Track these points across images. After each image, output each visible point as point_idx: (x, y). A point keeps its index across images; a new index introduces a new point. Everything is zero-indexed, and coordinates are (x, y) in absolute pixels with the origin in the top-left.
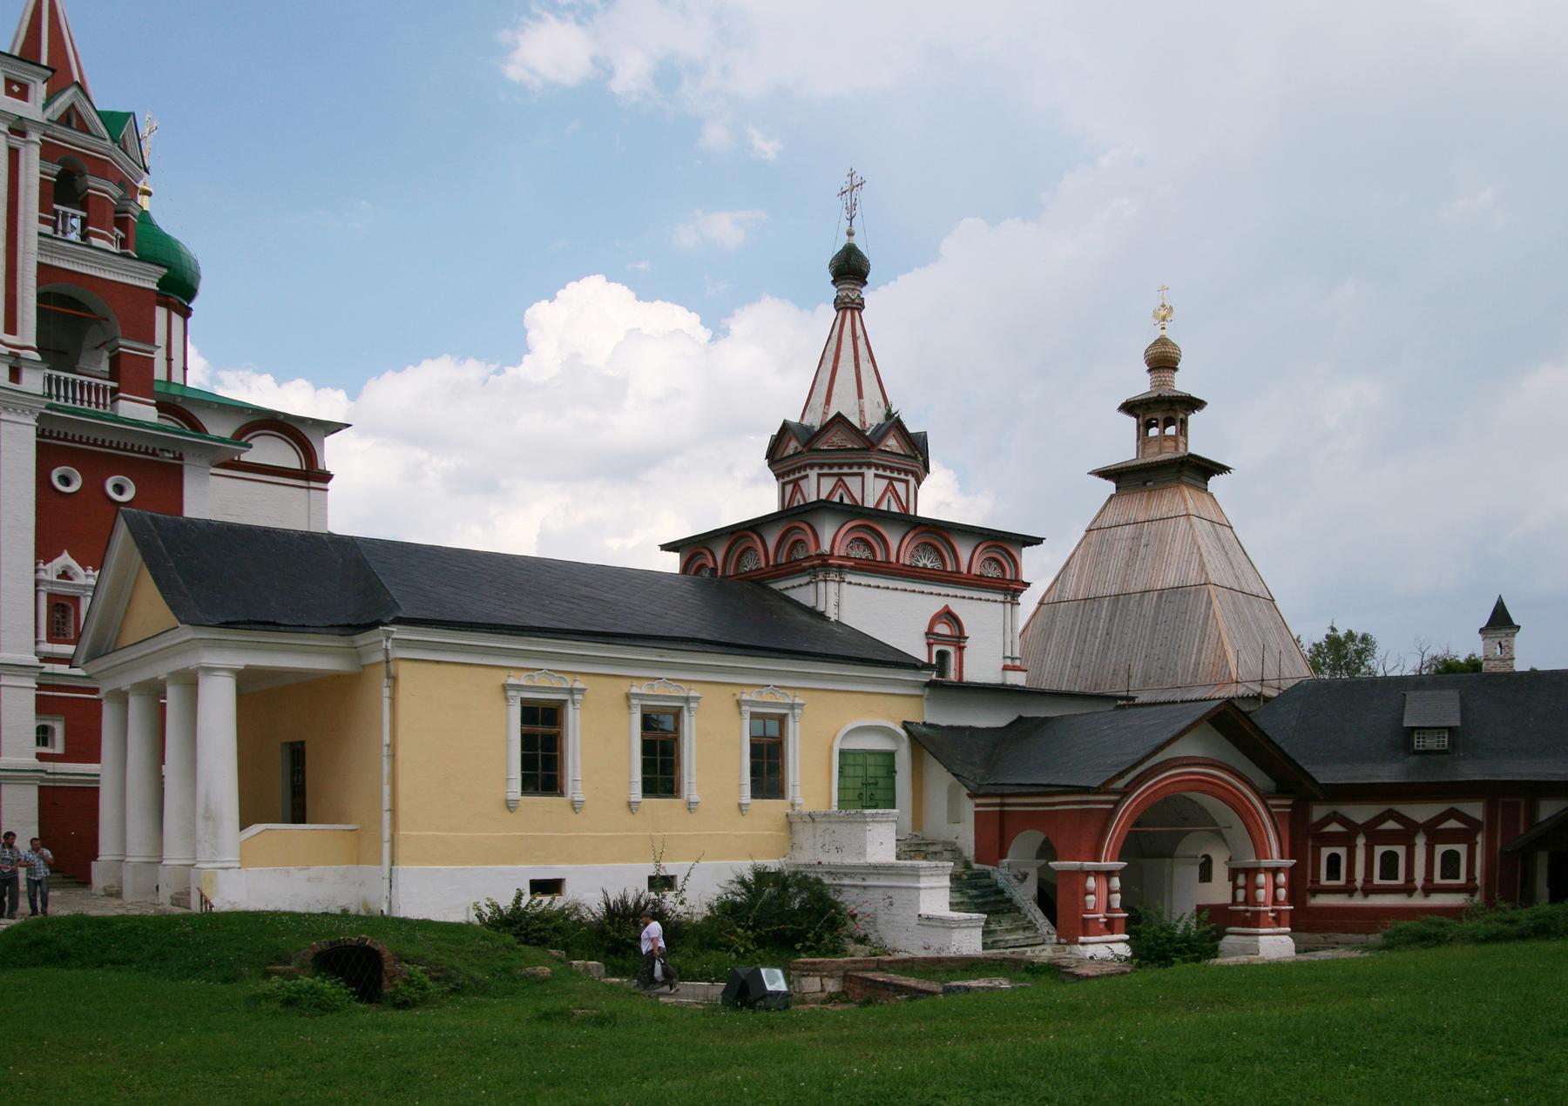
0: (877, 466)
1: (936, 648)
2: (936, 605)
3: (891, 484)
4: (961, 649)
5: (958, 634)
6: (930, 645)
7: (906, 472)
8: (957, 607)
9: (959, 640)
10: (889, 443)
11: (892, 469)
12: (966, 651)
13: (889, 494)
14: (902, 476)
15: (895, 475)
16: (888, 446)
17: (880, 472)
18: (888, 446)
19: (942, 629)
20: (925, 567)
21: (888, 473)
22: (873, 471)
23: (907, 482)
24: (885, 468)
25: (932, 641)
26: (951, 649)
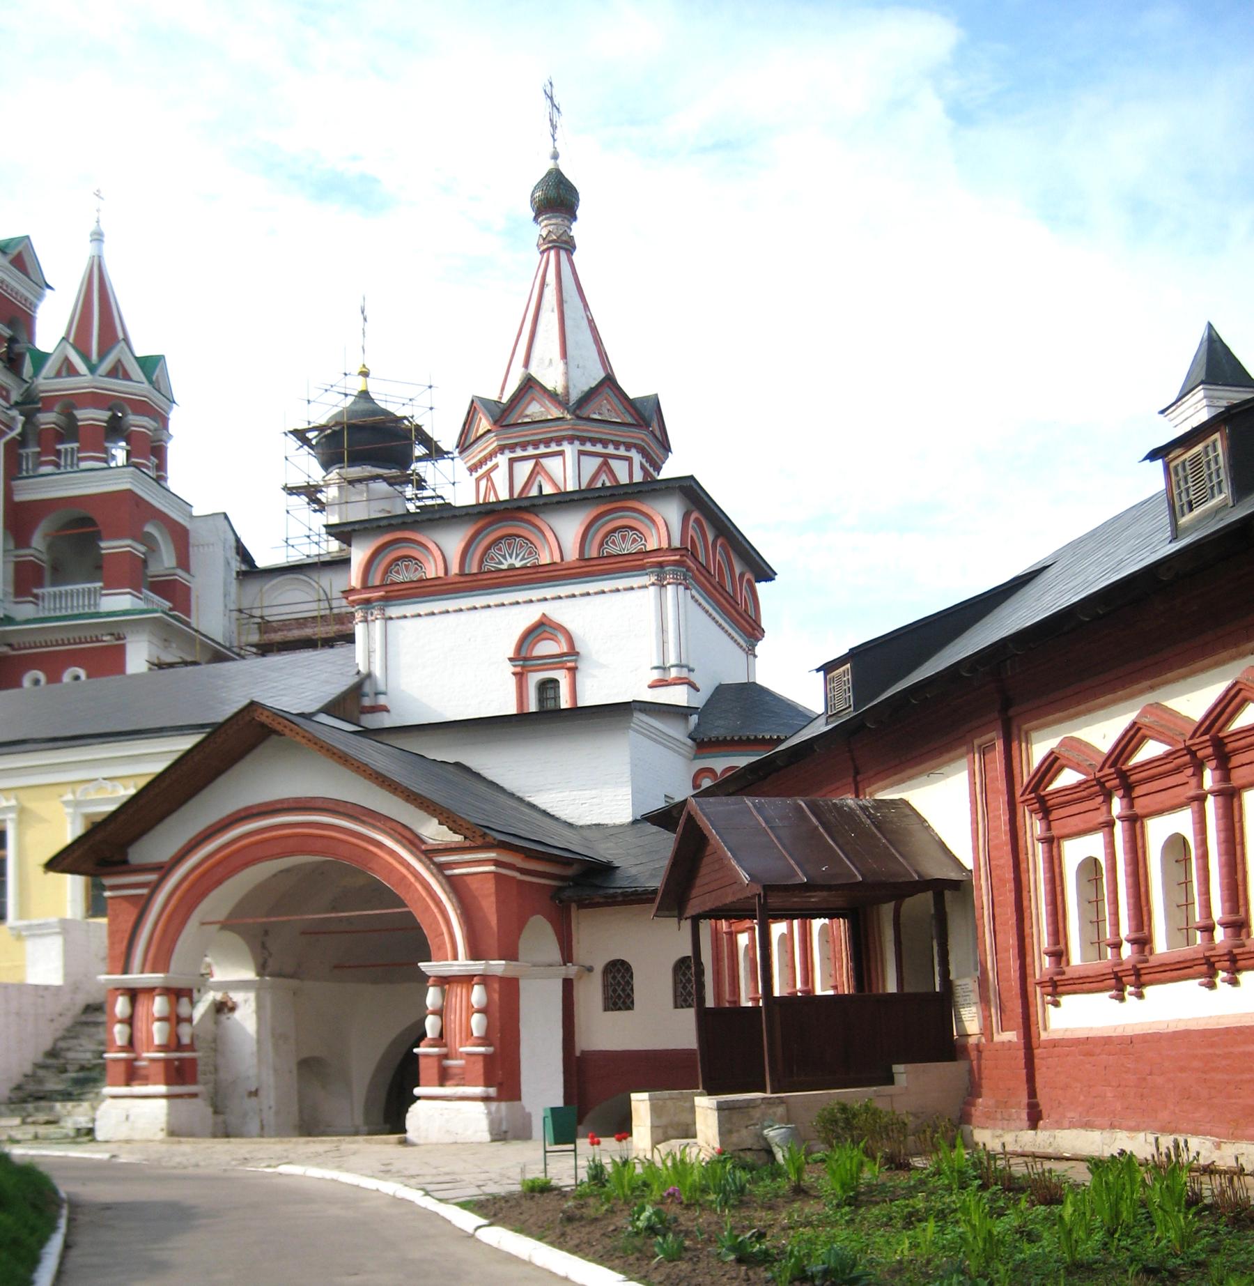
0: (512, 448)
1: (534, 678)
2: (529, 616)
3: (536, 464)
4: (573, 670)
5: (565, 650)
6: (520, 677)
7: (559, 441)
8: (562, 613)
9: (571, 658)
10: (528, 412)
11: (536, 444)
12: (579, 676)
13: (539, 478)
14: (554, 448)
15: (542, 450)
16: (527, 416)
17: (519, 453)
18: (527, 416)
19: (546, 648)
20: (512, 568)
21: (531, 451)
22: (508, 455)
23: (561, 453)
24: (524, 446)
25: (518, 670)
26: (562, 676)
